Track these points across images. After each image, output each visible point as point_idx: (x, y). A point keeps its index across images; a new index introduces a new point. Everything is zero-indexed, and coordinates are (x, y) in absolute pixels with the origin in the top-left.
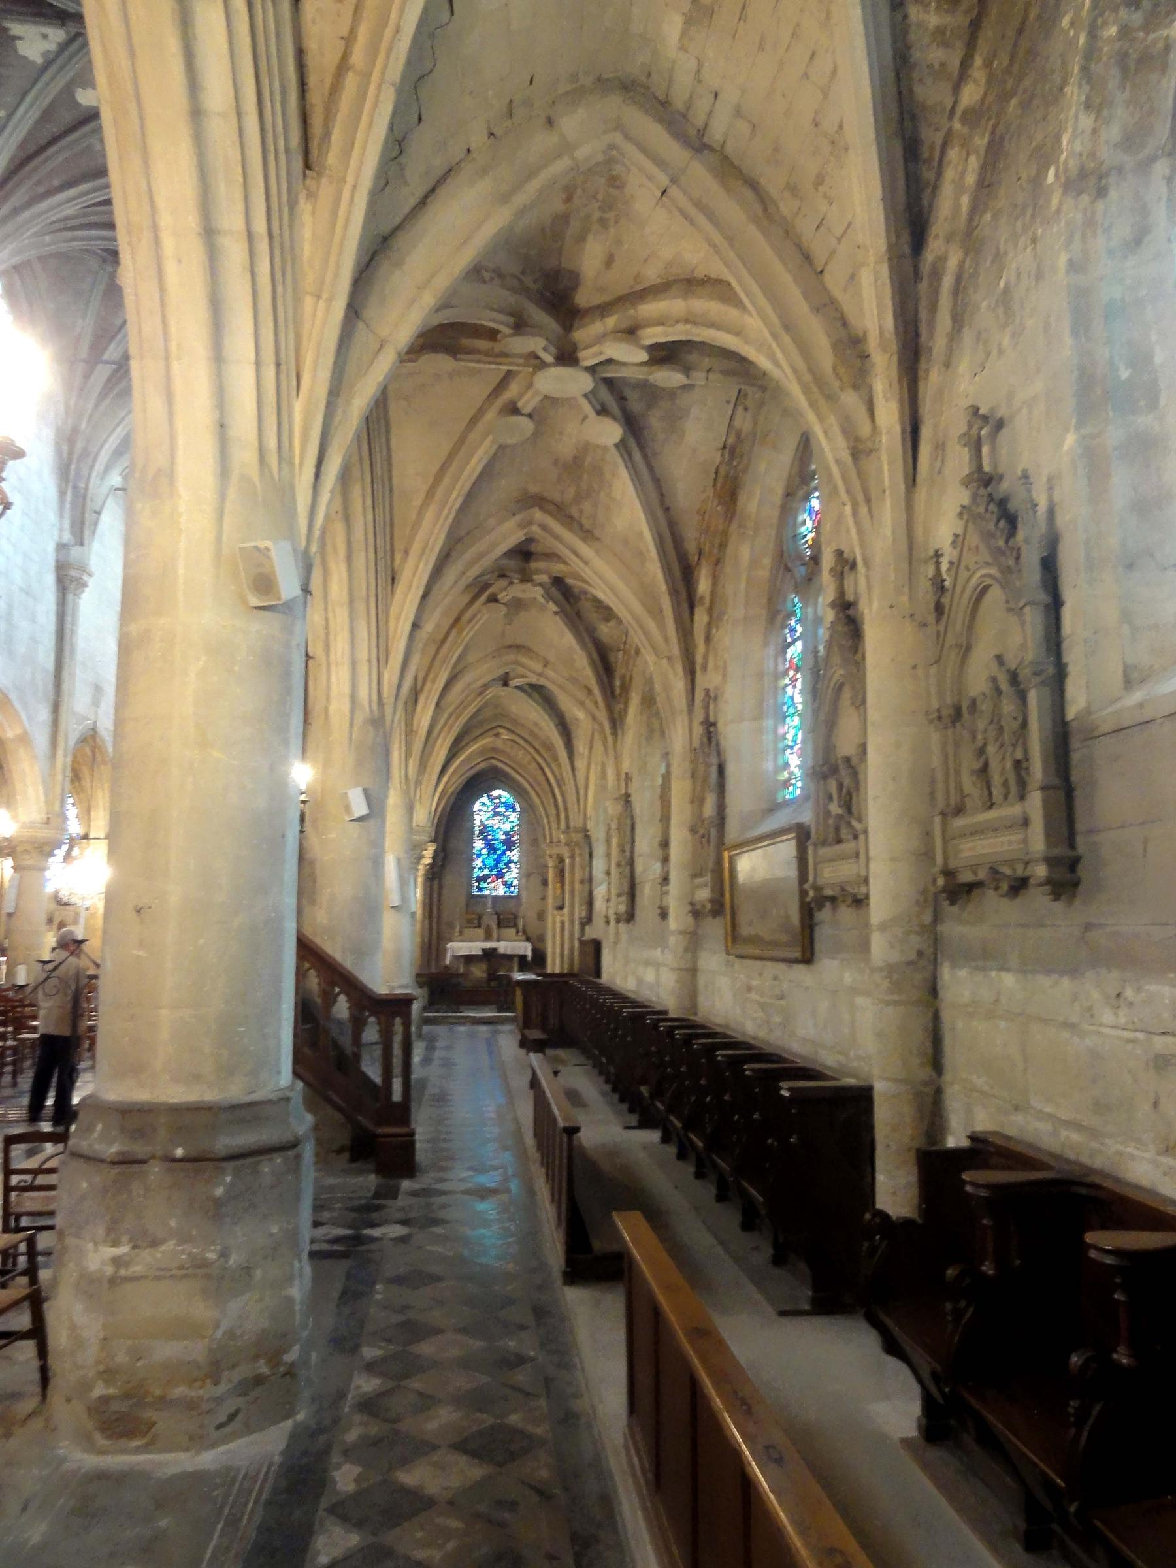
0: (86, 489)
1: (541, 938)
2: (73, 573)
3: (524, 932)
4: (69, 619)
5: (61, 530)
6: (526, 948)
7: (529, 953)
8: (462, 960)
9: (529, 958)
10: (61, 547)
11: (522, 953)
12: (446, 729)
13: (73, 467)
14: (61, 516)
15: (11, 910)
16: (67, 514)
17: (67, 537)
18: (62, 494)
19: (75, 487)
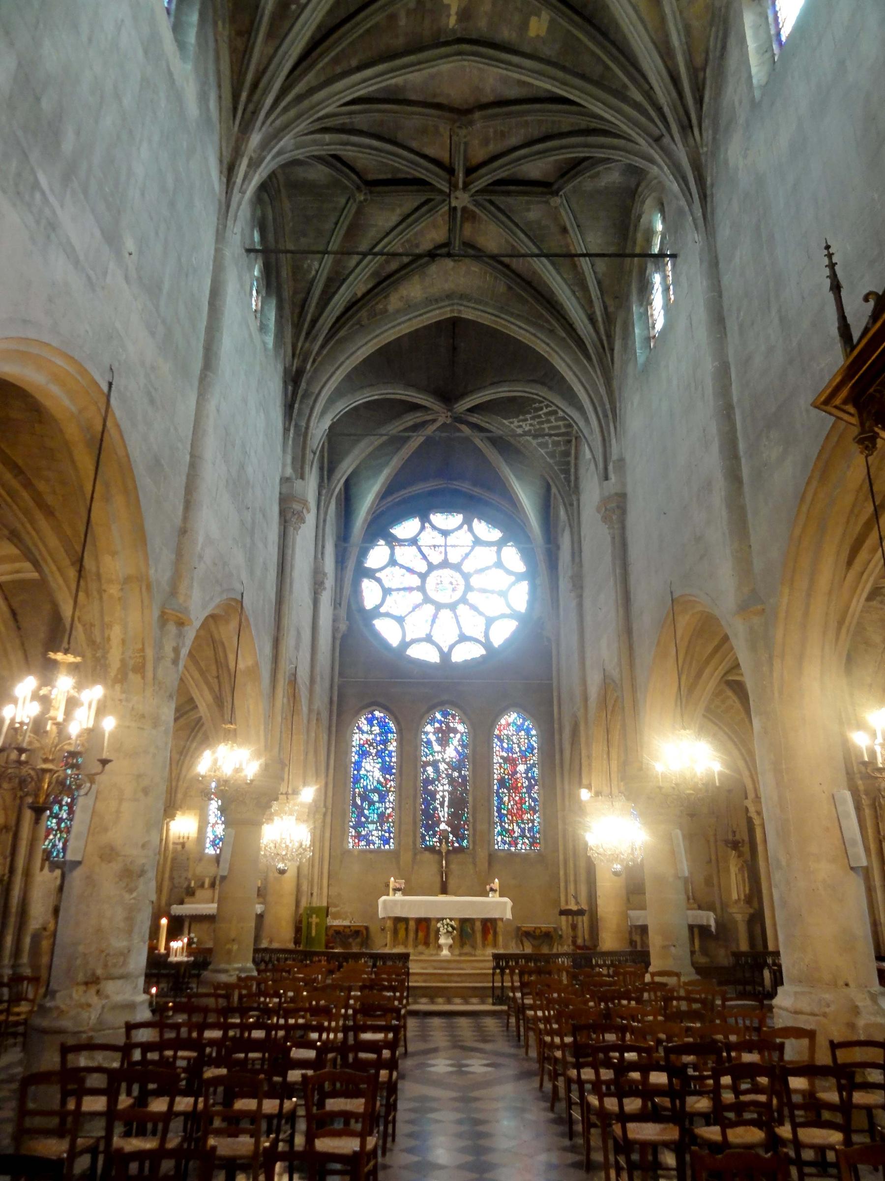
0: (307, 428)
1: (724, 906)
2: (296, 506)
3: (694, 899)
4: (289, 552)
5: (284, 466)
6: (708, 919)
7: (712, 923)
8: (639, 931)
9: (713, 929)
10: (285, 480)
11: (705, 923)
12: (718, 655)
13: (296, 406)
14: (284, 451)
15: (225, 874)
16: (289, 450)
17: (289, 471)
18: (286, 430)
19: (296, 426)
